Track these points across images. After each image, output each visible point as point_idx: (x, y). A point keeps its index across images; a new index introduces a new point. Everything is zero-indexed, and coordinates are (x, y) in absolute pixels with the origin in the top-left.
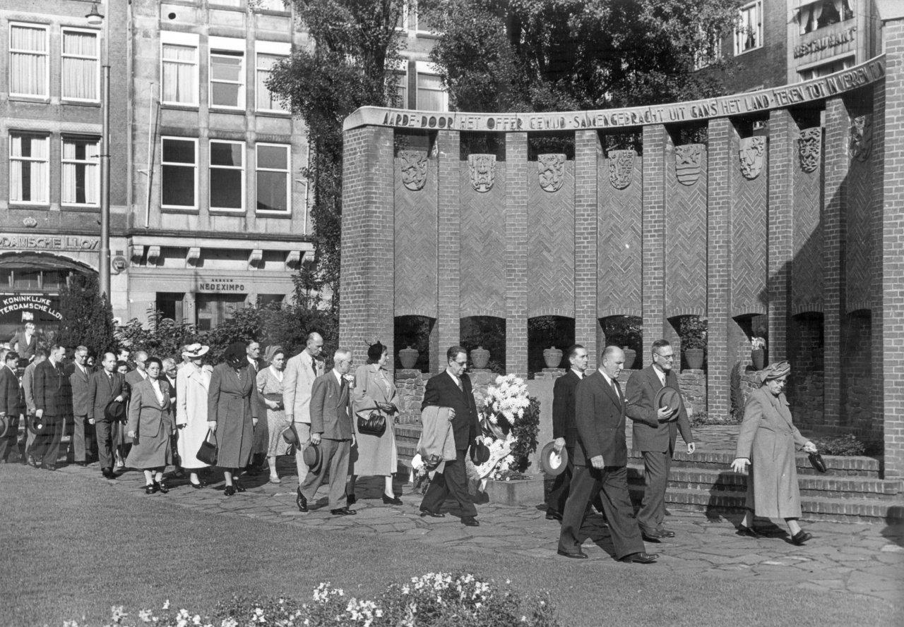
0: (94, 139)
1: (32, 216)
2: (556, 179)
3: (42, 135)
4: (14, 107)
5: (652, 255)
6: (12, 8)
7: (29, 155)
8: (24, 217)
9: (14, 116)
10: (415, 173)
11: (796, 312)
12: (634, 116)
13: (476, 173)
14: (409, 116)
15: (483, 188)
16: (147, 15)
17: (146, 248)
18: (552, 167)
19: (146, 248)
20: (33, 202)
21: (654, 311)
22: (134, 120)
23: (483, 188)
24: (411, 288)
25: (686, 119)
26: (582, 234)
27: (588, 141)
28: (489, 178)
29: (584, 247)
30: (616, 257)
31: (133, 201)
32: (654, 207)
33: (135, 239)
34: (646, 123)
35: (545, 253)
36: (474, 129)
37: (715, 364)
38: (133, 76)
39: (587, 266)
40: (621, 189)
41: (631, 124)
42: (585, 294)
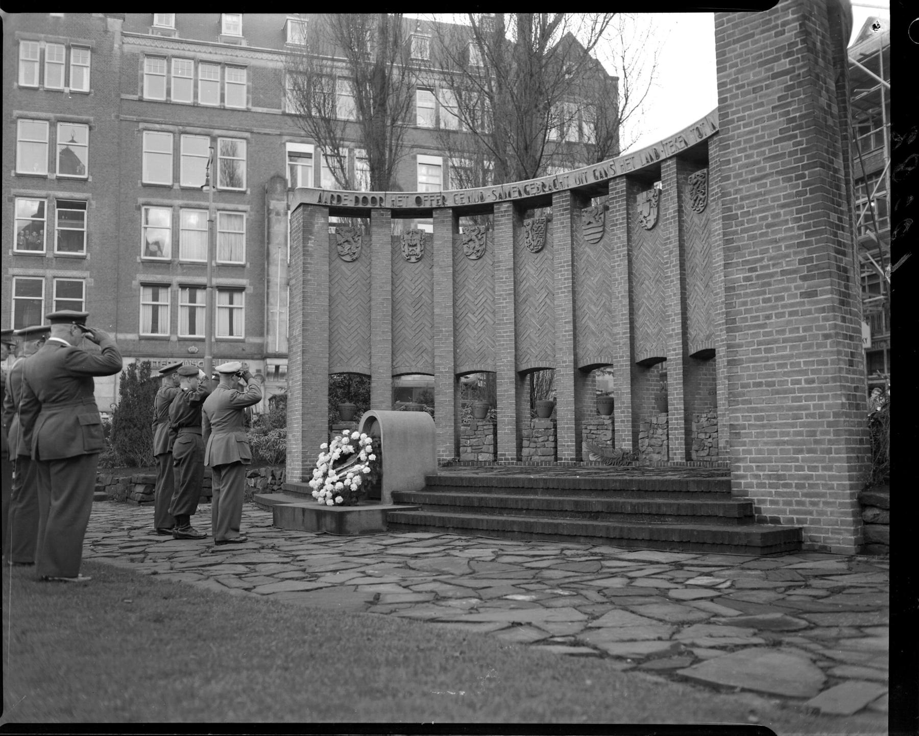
0: (241, 289)
1: (195, 345)
2: (477, 248)
3: (203, 287)
4: (183, 269)
5: (563, 310)
6: (182, 199)
7: (195, 302)
8: (188, 346)
9: (183, 274)
10: (349, 246)
11: (693, 351)
12: (544, 185)
13: (406, 246)
14: (342, 195)
15: (413, 259)
16: (278, 200)
17: (277, 367)
18: (474, 237)
19: (277, 367)
20: (197, 336)
21: (565, 362)
22: (268, 275)
23: (413, 259)
24: (346, 348)
25: (589, 183)
26: (501, 295)
27: (505, 211)
28: (418, 250)
29: (503, 307)
30: (532, 315)
31: (268, 333)
32: (562, 267)
33: (269, 361)
34: (555, 191)
35: (469, 315)
36: (404, 207)
37: (620, 408)
38: (268, 243)
39: (506, 324)
40: (537, 252)
41: (542, 193)
42: (504, 349)
